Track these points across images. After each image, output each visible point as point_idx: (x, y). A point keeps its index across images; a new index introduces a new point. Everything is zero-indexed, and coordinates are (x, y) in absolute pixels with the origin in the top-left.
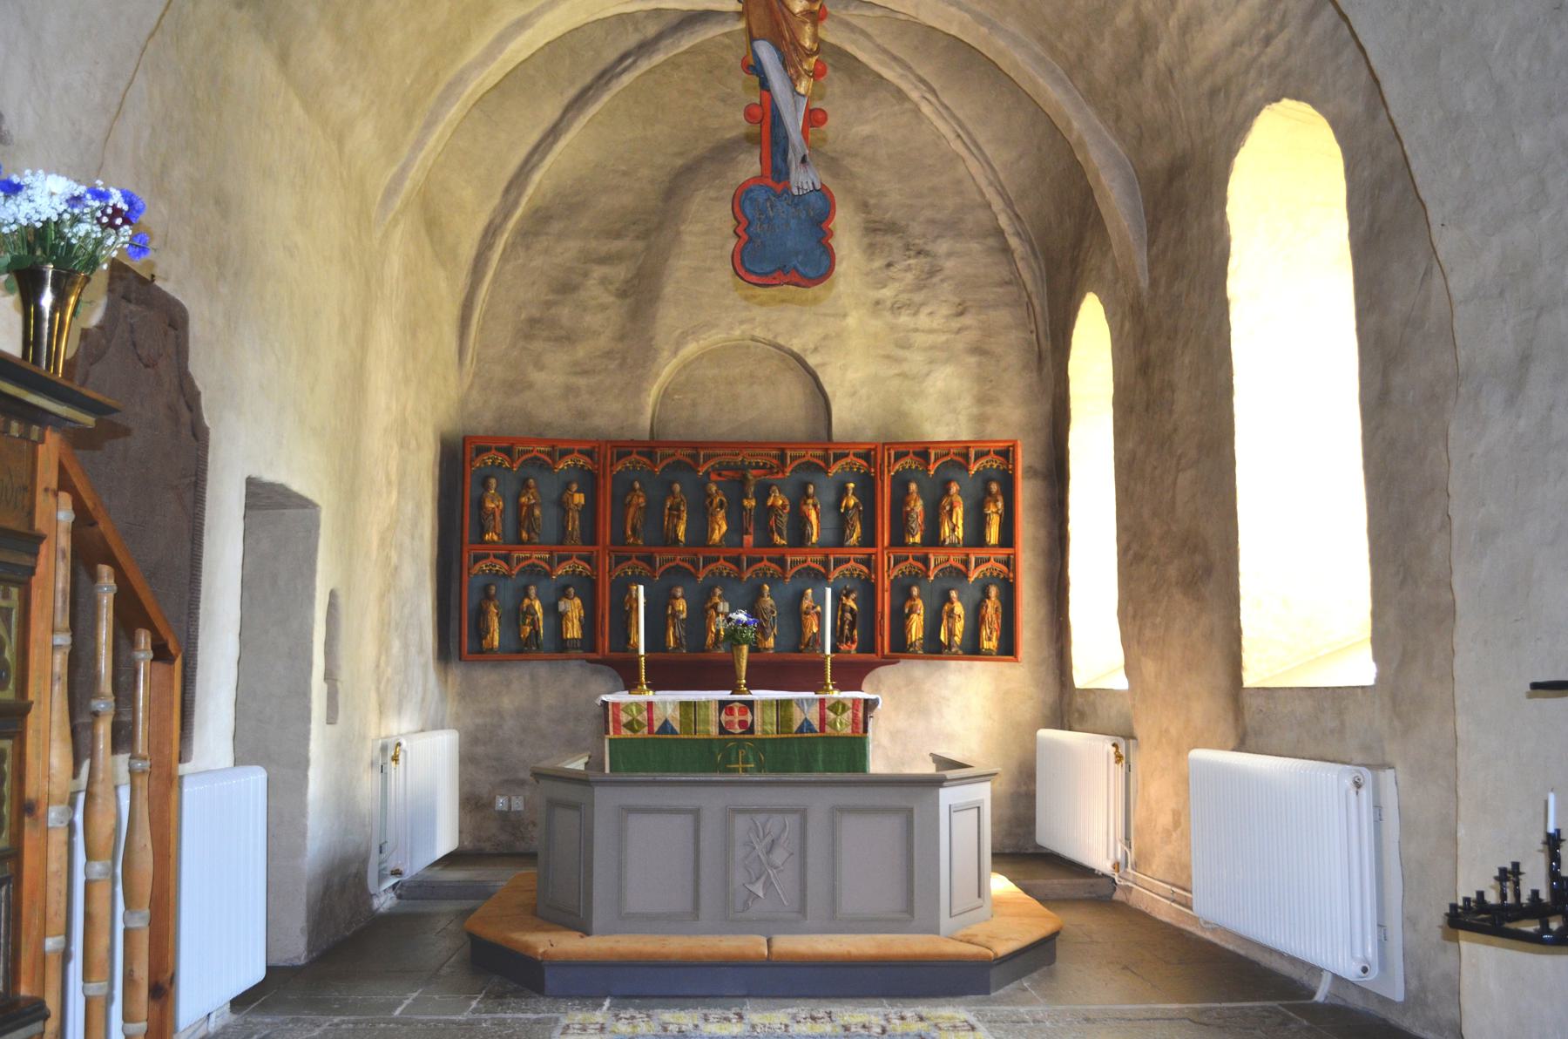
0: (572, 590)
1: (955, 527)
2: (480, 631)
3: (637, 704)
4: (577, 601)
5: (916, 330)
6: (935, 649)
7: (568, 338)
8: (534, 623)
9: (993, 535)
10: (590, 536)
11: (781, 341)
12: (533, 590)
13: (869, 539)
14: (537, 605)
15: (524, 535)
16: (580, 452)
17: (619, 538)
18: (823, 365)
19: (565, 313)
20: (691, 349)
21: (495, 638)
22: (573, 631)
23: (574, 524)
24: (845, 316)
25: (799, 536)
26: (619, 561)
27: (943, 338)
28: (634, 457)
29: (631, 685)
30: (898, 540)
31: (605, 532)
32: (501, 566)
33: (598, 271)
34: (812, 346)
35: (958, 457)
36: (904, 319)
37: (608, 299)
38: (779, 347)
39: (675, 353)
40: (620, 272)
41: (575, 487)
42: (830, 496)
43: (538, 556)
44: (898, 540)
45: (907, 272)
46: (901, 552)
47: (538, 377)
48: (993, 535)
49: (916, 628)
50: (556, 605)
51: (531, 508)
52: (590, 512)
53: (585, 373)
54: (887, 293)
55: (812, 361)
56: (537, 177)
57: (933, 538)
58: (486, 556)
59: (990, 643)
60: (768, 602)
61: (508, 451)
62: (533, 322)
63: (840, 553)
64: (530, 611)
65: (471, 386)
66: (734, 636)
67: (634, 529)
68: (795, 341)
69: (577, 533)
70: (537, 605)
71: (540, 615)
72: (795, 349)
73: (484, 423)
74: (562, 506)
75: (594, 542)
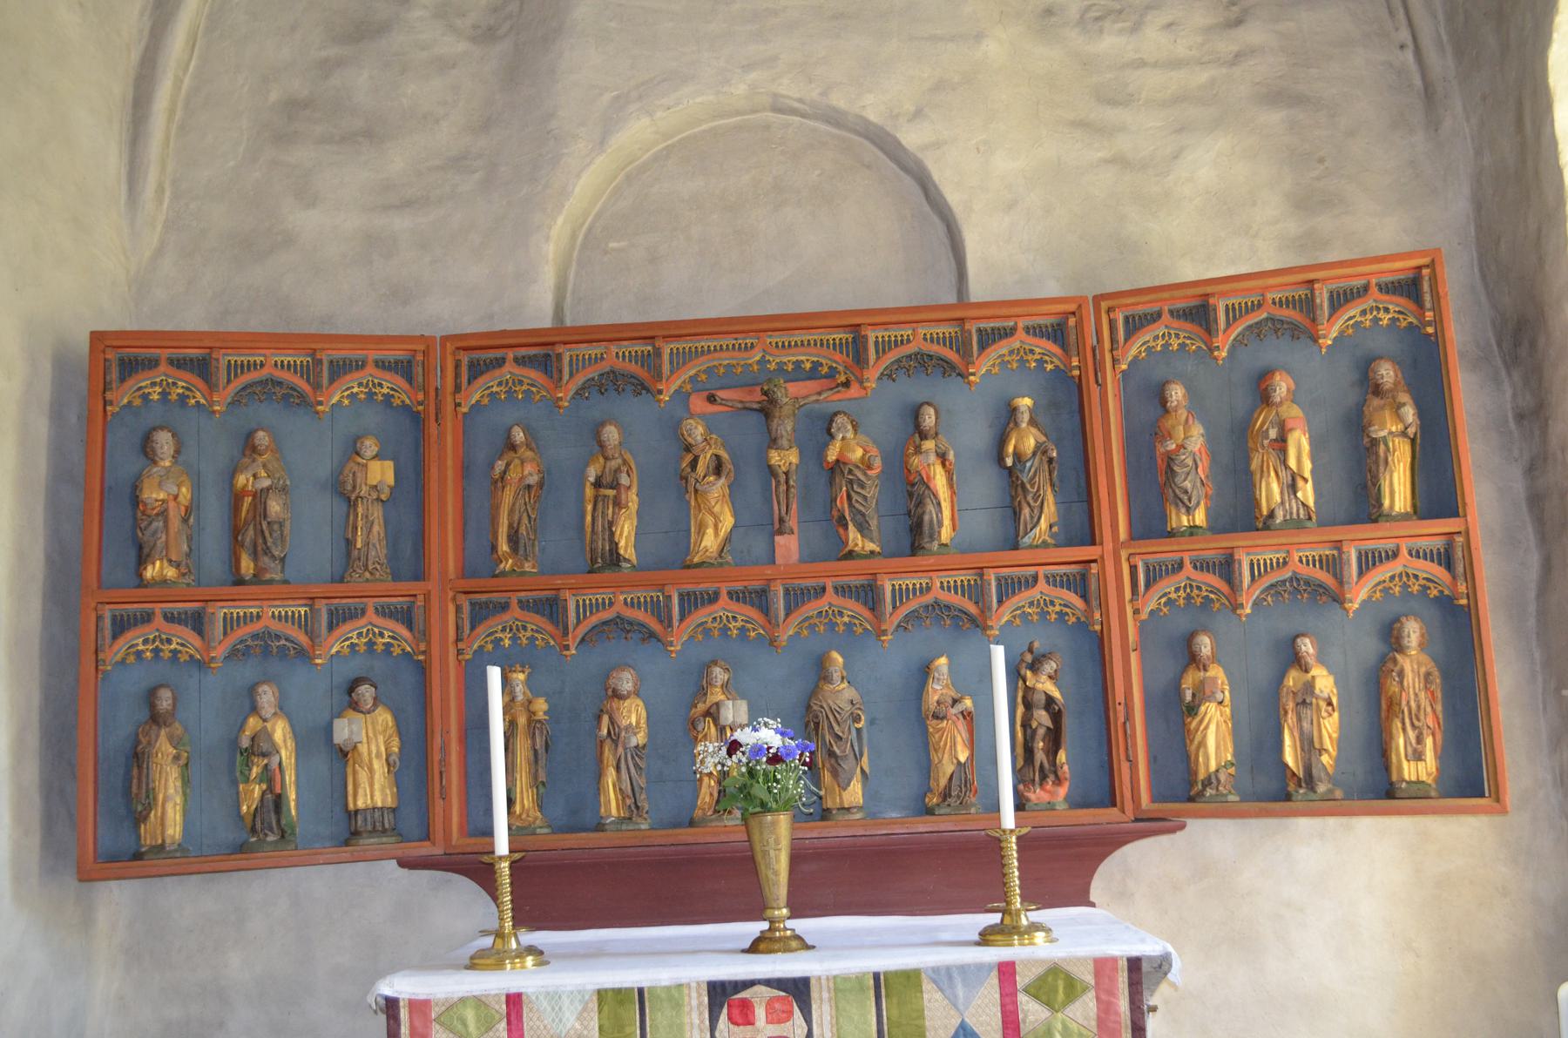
0: (366, 692)
1: (1295, 476)
2: (133, 802)
3: (479, 1002)
4: (384, 717)
5: (1141, 64)
6: (1275, 788)
7: (372, 134)
8: (268, 776)
9: (1398, 489)
10: (411, 559)
11: (839, 100)
12: (267, 697)
13: (1082, 527)
14: (280, 732)
15: (247, 566)
16: (381, 365)
18: (937, 145)
19: (361, 81)
20: (638, 132)
21: (171, 817)
22: (373, 788)
23: (372, 531)
24: (979, 37)
25: (914, 534)
26: (481, 613)
27: (1203, 76)
28: (509, 371)
30: (1150, 524)
31: (446, 552)
32: (183, 639)
34: (909, 107)
35: (1293, 308)
36: (1110, 43)
37: (453, 46)
38: (834, 118)
39: (602, 143)
41: (370, 447)
42: (974, 434)
44: (1150, 524)
46: (1163, 551)
47: (306, 221)
48: (1398, 489)
49: (1216, 740)
50: (328, 730)
51: (260, 497)
53: (407, 204)
55: (911, 138)
57: (1242, 514)
58: (147, 618)
59: (1418, 765)
60: (841, 694)
61: (202, 368)
62: (294, 106)
63: (1011, 564)
64: (260, 748)
65: (159, 252)
66: (746, 793)
67: (514, 539)
68: (869, 99)
69: (379, 552)
70: (280, 732)
71: (287, 755)
72: (872, 116)
74: (345, 495)
75: (420, 575)
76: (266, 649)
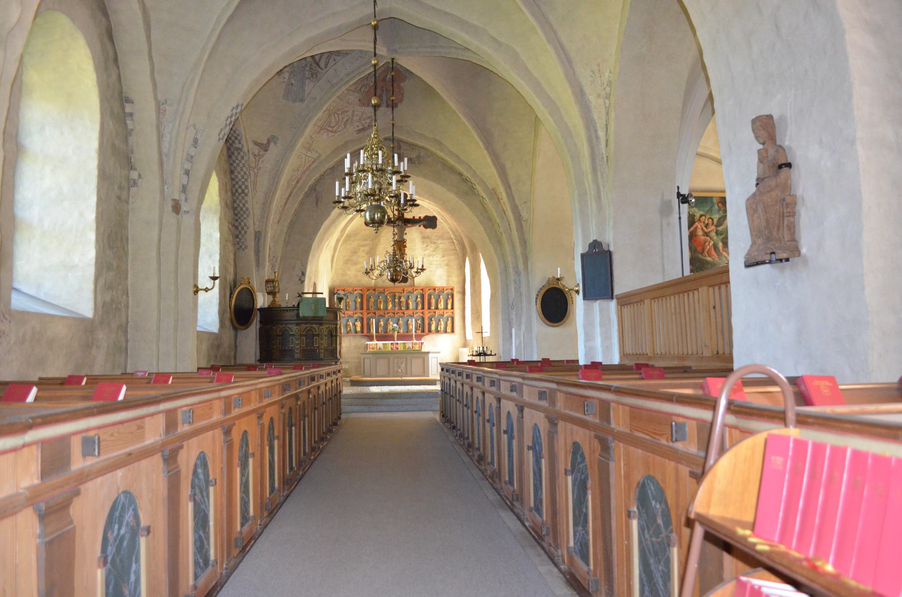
1: (441, 305)
6: (437, 331)
7: (356, 264)
9: (449, 307)
13: (423, 308)
17: (368, 309)
19: (354, 258)
22: (359, 329)
23: (358, 306)
25: (408, 308)
29: (372, 340)
30: (429, 308)
31: (365, 307)
33: (362, 248)
35: (442, 290)
36: (431, 258)
40: (367, 249)
42: (414, 299)
43: (351, 313)
44: (429, 308)
45: (431, 247)
47: (349, 273)
48: (449, 307)
49: (433, 327)
52: (362, 303)
54: (427, 252)
56: (348, 229)
57: (437, 308)
59: (449, 330)
60: (401, 322)
62: (347, 260)
66: (394, 330)
73: (337, 283)
74: (356, 302)
76: (350, 316)
